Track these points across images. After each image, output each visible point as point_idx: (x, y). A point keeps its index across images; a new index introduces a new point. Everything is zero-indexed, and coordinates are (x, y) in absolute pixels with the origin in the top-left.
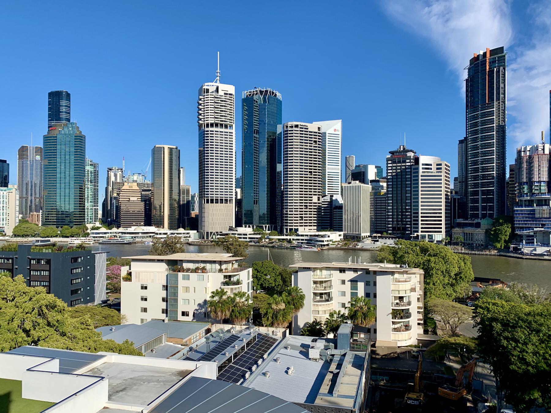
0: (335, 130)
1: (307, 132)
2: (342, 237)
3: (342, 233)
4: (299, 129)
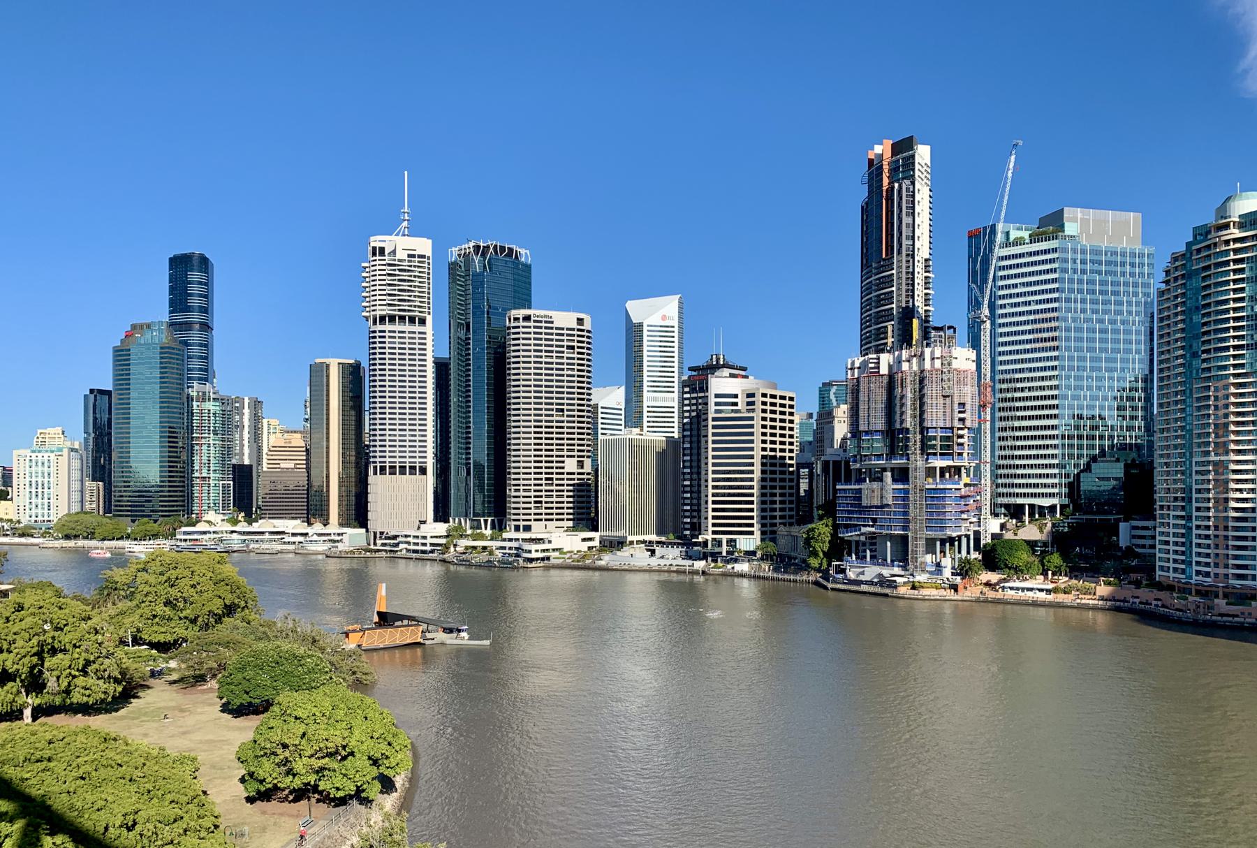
0: (664, 318)
2: (596, 543)
4: (532, 324)
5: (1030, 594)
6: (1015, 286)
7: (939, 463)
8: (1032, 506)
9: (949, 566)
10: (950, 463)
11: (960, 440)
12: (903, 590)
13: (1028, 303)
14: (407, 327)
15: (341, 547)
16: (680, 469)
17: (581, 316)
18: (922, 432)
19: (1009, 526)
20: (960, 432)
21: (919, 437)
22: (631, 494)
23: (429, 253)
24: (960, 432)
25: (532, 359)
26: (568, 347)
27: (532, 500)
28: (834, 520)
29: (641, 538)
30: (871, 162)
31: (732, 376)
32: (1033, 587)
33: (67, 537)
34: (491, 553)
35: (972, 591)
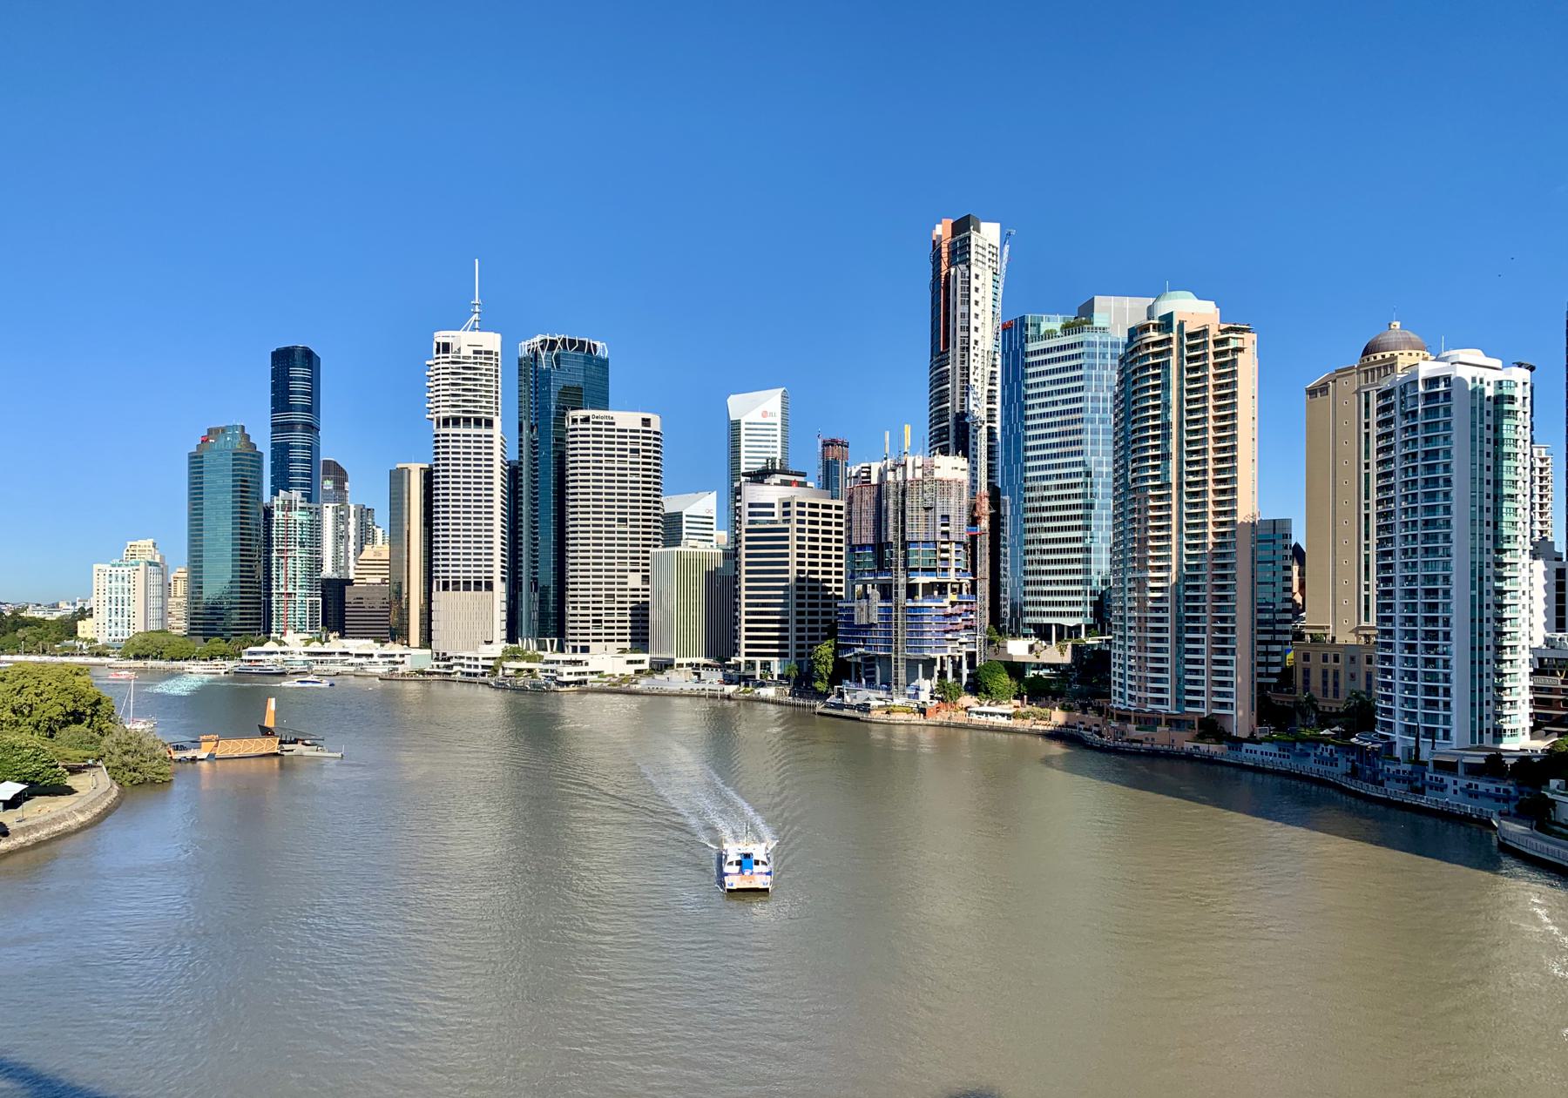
0: (765, 414)
2: (646, 666)
3: (646, 657)
4: (590, 426)
5: (991, 719)
6: (1044, 384)
7: (921, 580)
8: (1060, 627)
9: (928, 689)
10: (934, 579)
12: (877, 715)
13: (1055, 403)
14: (473, 430)
15: (401, 669)
16: (721, 589)
17: (647, 416)
23: (497, 348)
26: (632, 451)
29: (689, 660)
31: (784, 483)
32: (1002, 712)
33: (137, 657)
34: (534, 676)
35: (943, 716)
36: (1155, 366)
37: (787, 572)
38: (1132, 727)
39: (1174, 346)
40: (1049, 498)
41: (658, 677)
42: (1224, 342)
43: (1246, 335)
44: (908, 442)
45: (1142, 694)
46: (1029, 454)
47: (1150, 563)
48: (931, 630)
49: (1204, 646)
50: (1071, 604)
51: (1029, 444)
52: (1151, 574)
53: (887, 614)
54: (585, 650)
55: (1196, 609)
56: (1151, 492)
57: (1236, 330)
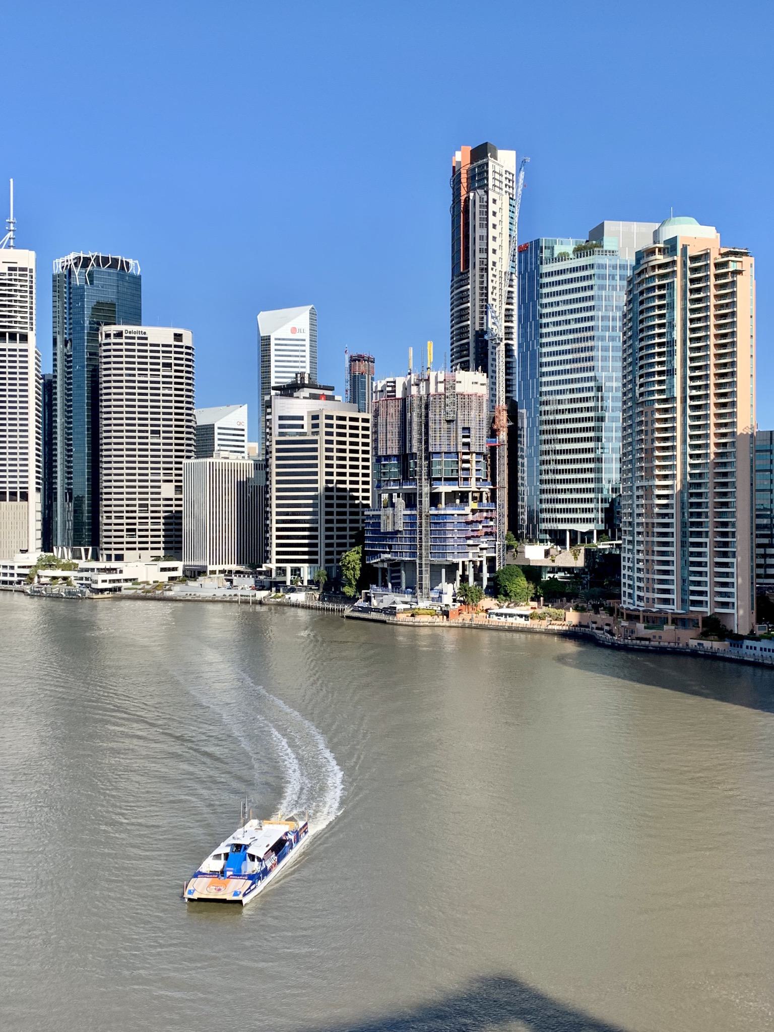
0: (294, 330)
1: (146, 345)
2: (179, 573)
3: (179, 565)
4: (123, 340)
5: (510, 620)
6: (558, 304)
7: (444, 488)
8: (574, 533)
9: (451, 592)
10: (456, 488)
11: (466, 465)
12: (401, 617)
13: (568, 322)
17: (179, 331)
18: (428, 458)
19: (552, 552)
20: (465, 457)
21: (425, 463)
22: (213, 523)
23: (31, 265)
24: (465, 457)
25: (124, 378)
26: (165, 365)
27: (125, 527)
28: (363, 548)
30: (454, 167)
31: (314, 397)
32: (521, 613)
35: (466, 617)
36: (661, 287)
37: (316, 482)
38: (640, 626)
39: (678, 268)
40: (563, 411)
41: (191, 584)
42: (725, 264)
43: (744, 259)
44: (430, 358)
45: (650, 595)
46: (544, 369)
47: (657, 472)
48: (454, 536)
49: (707, 550)
50: (584, 510)
51: (544, 360)
52: (658, 482)
53: (412, 522)
54: (119, 558)
55: (699, 515)
56: (657, 406)
57: (736, 254)
